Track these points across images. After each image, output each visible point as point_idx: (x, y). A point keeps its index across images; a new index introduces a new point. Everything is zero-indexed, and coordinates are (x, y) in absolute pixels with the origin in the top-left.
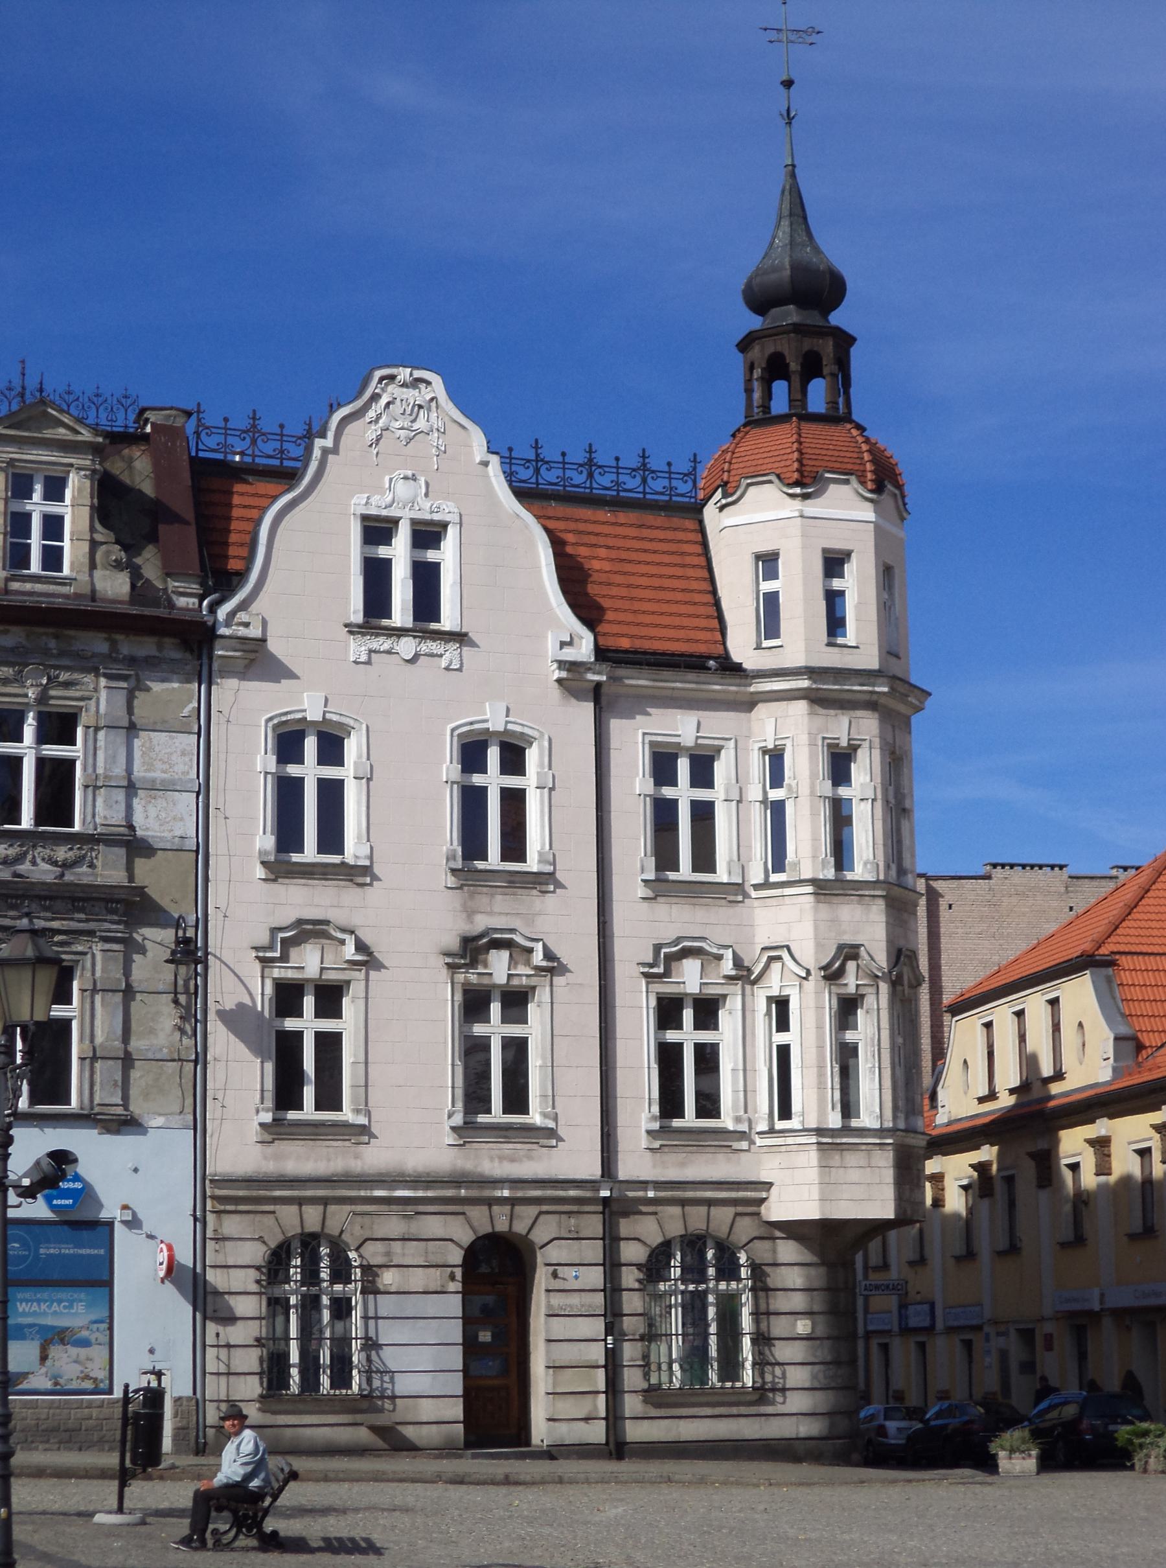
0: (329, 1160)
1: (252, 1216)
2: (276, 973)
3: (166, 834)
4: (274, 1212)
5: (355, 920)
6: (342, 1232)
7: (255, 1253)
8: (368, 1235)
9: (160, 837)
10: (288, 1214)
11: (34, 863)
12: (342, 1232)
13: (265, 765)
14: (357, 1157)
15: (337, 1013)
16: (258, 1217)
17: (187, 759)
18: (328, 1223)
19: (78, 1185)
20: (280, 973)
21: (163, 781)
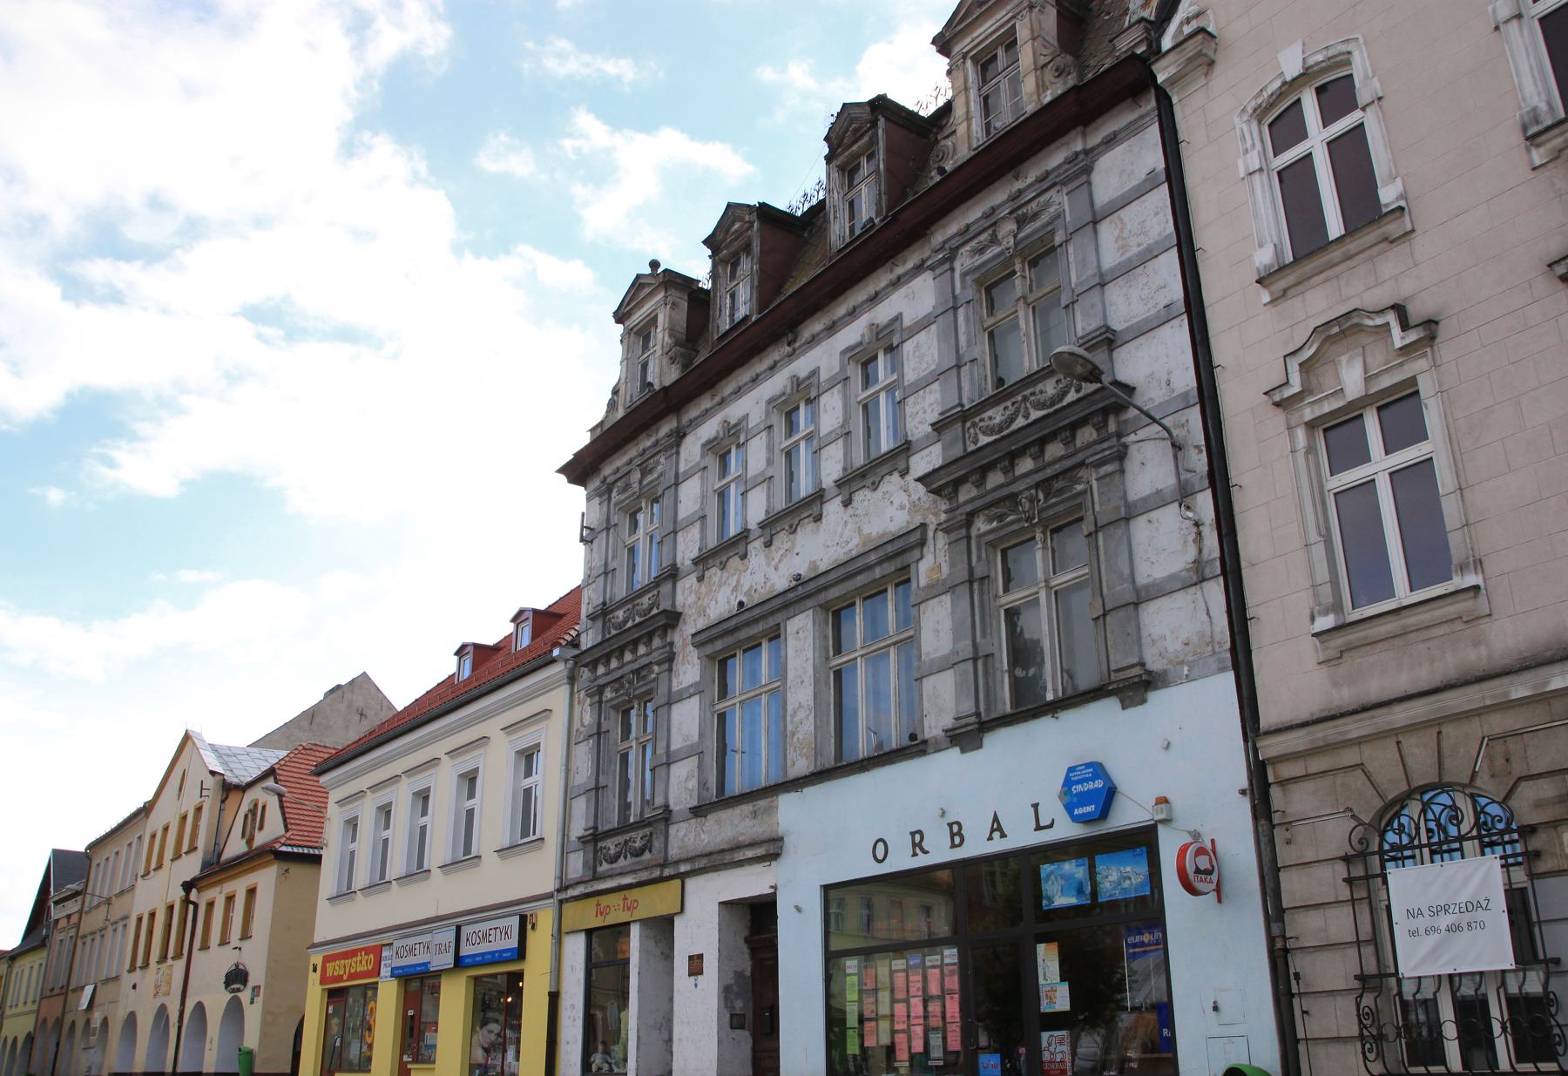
0: (1433, 661)
1: (1329, 779)
2: (1309, 414)
3: (1153, 311)
4: (1360, 765)
5: (1403, 289)
6: (1474, 774)
7: (1336, 835)
8: (1519, 769)
9: (1144, 320)
10: (1382, 760)
12: (1474, 774)
13: (1247, 167)
14: (1476, 644)
15: (1418, 433)
16: (1340, 779)
17: (1161, 214)
18: (1448, 763)
19: (1099, 784)
20: (1313, 412)
21: (1139, 254)
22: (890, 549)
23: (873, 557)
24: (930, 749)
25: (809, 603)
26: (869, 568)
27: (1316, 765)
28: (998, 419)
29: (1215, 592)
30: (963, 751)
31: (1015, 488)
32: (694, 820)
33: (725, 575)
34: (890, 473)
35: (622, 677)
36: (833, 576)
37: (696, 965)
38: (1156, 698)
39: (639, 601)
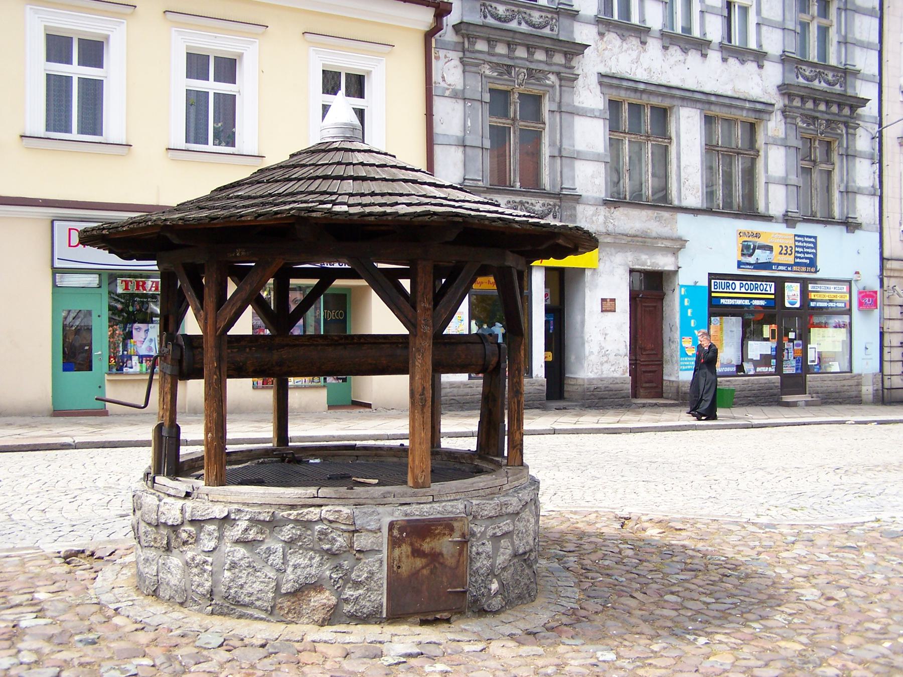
11: (820, 82)
22: (759, 106)
23: (747, 105)
24: (774, 220)
25: (699, 105)
26: (742, 108)
27: (896, 274)
28: (807, 73)
29: (877, 199)
30: (788, 227)
31: (818, 115)
32: (602, 208)
33: (625, 46)
34: (752, 61)
35: (514, 67)
36: (721, 100)
37: (608, 306)
38: (857, 232)
39: (528, 11)
